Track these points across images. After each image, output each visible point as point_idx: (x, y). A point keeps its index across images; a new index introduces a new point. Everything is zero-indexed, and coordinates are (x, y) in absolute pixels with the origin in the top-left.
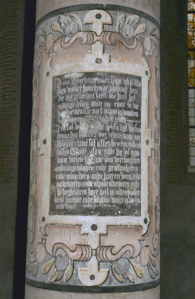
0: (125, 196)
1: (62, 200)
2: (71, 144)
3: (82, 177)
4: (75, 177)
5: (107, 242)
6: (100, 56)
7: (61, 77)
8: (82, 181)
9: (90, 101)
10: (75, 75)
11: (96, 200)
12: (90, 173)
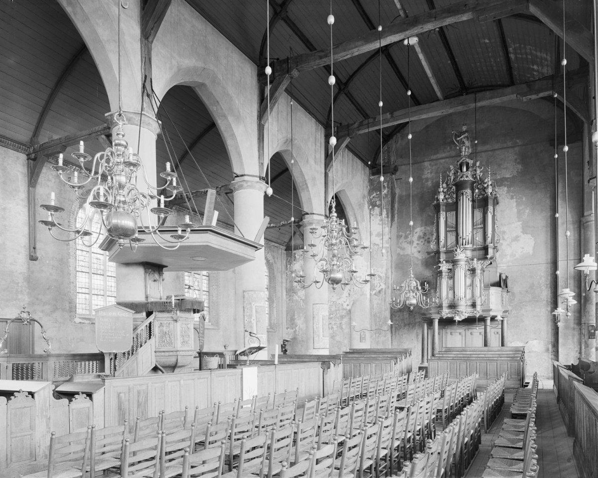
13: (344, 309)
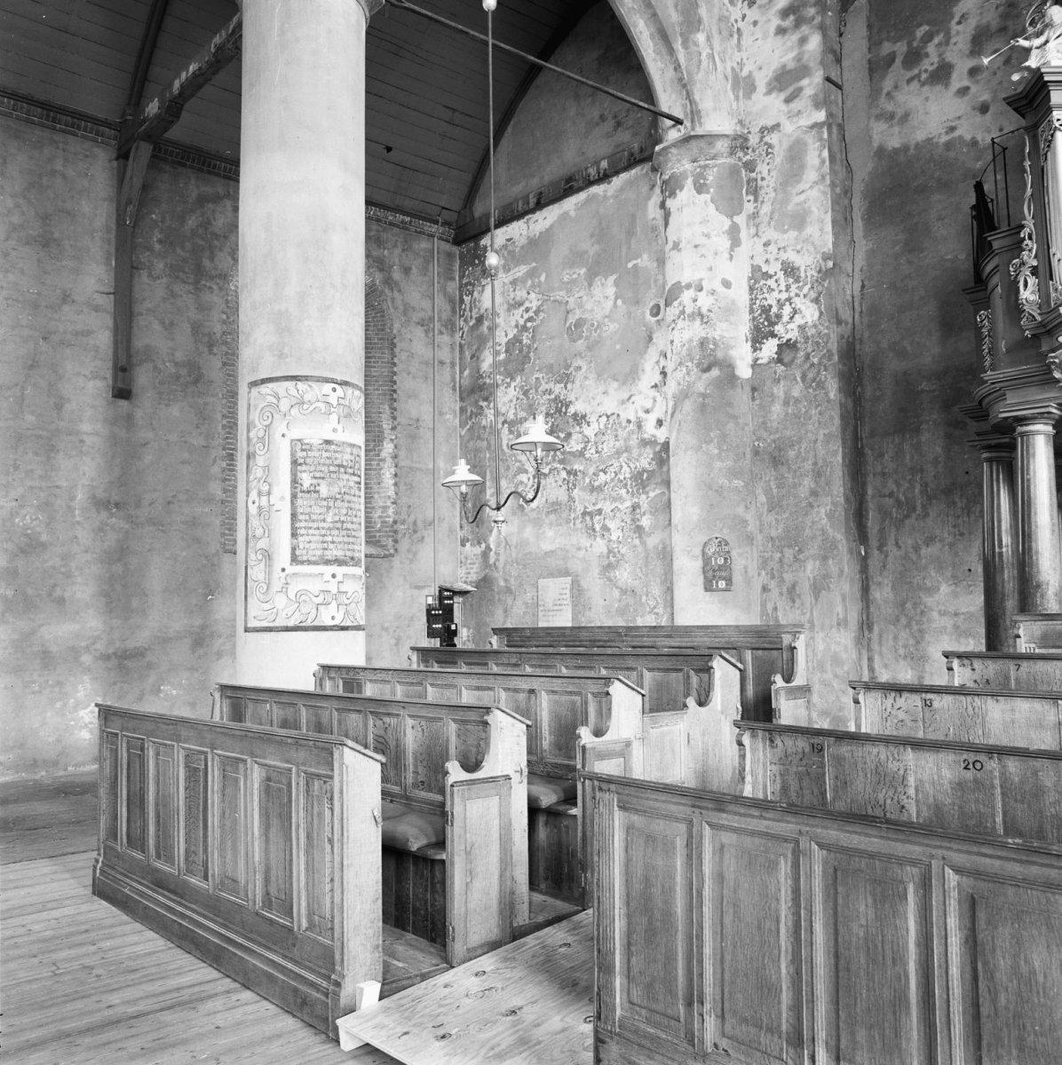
0: (354, 550)
1: (305, 552)
2: (313, 503)
3: (323, 532)
4: (317, 532)
5: (343, 588)
6: (337, 426)
7: (299, 440)
8: (324, 536)
9: (329, 466)
10: (316, 441)
11: (335, 552)
12: (329, 529)
13: (645, 443)
